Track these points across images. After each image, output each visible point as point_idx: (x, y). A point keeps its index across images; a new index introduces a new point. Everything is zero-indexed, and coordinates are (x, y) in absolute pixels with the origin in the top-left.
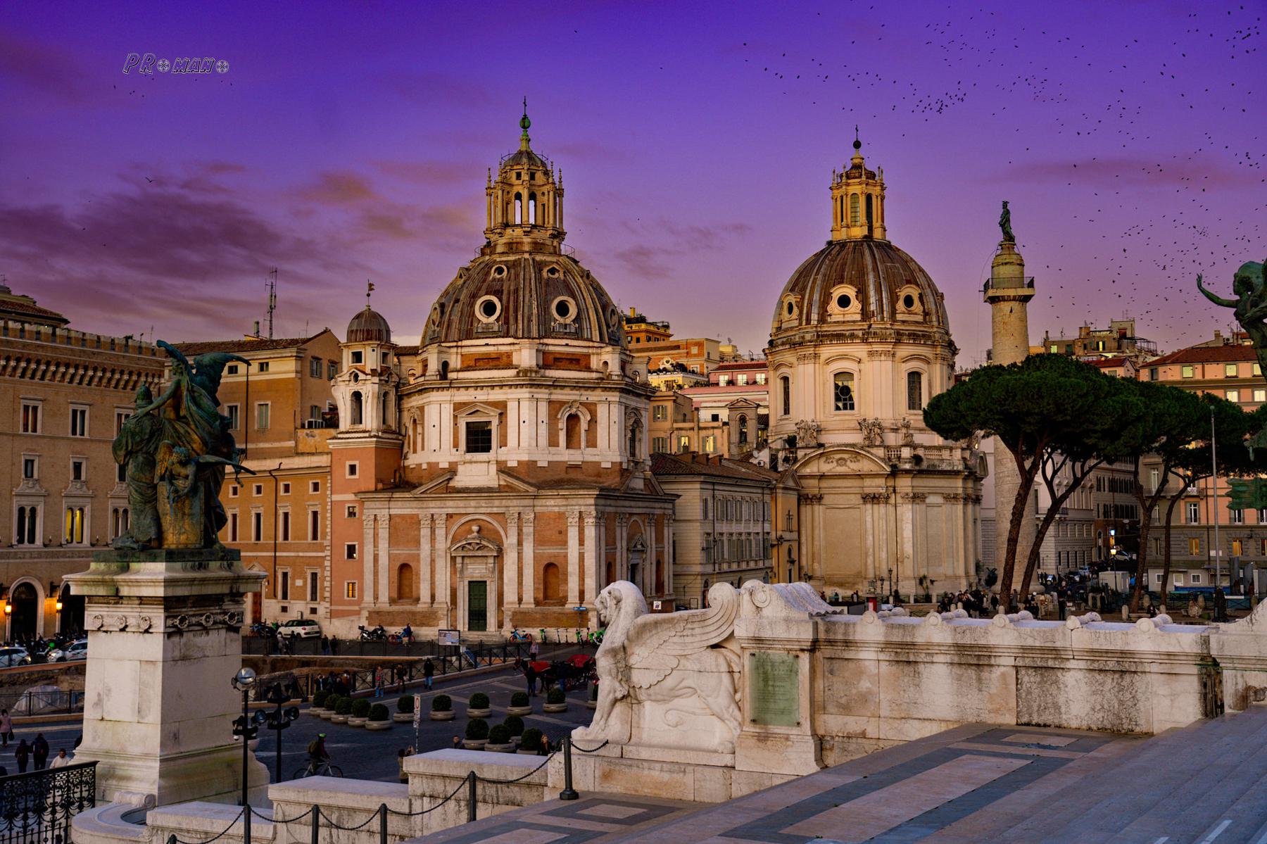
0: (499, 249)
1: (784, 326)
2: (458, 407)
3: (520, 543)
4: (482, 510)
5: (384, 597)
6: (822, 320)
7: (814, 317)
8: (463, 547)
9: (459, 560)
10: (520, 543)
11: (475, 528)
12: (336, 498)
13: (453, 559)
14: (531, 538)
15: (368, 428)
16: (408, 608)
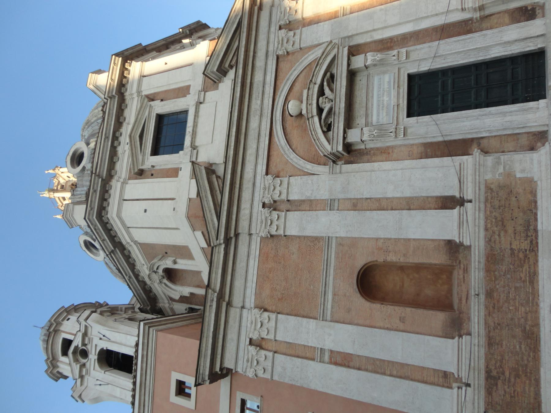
4: (268, 102)
8: (328, 128)
9: (354, 136)
16: (476, 276)
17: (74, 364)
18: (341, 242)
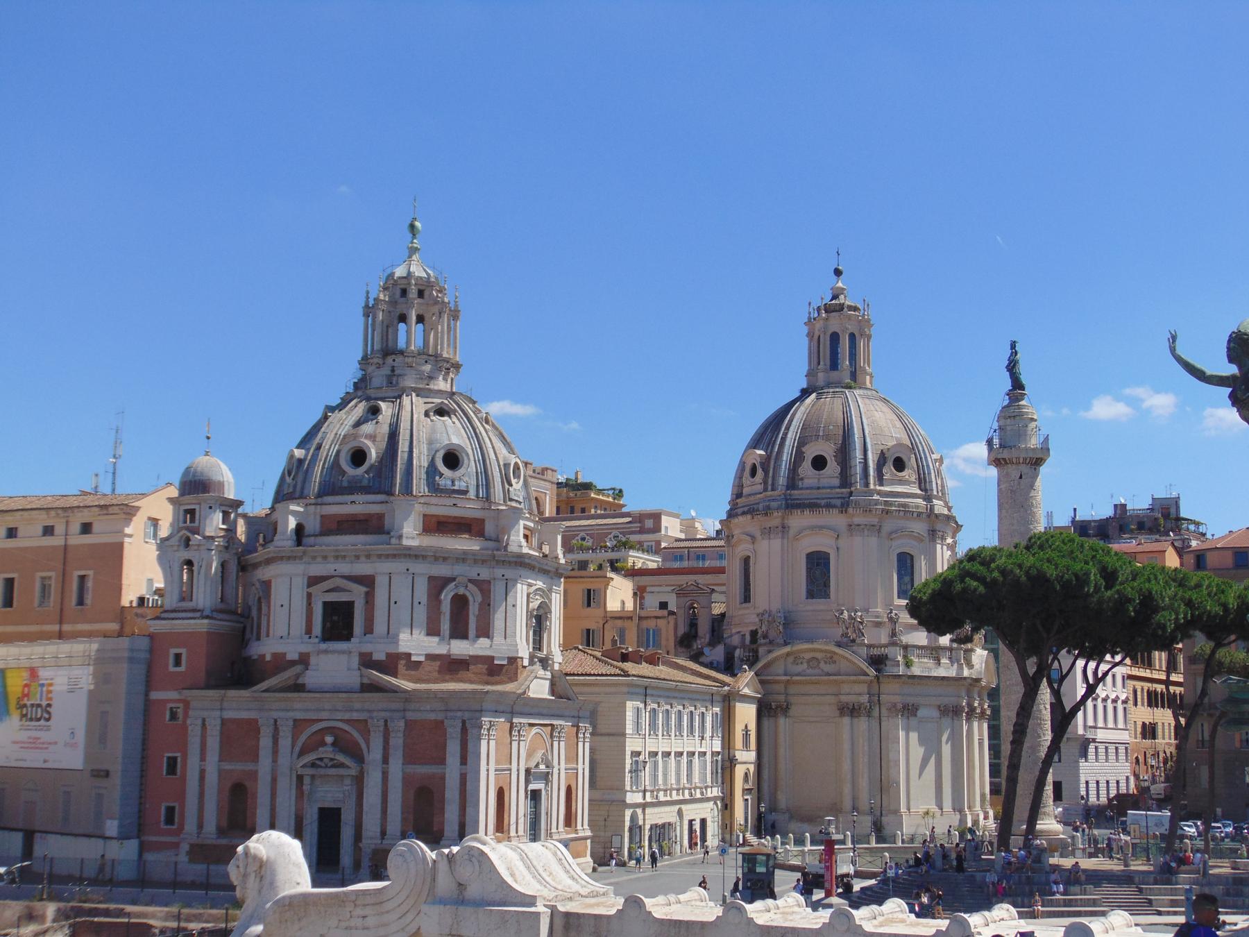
0: (376, 382)
1: (746, 491)
2: (313, 581)
3: (385, 760)
4: (339, 716)
5: (211, 826)
6: (793, 482)
7: (782, 481)
8: (313, 765)
9: (307, 780)
10: (385, 760)
11: (329, 739)
12: (155, 695)
13: (300, 778)
14: (400, 753)
15: (200, 606)
17: (177, 538)
18: (256, 772)
